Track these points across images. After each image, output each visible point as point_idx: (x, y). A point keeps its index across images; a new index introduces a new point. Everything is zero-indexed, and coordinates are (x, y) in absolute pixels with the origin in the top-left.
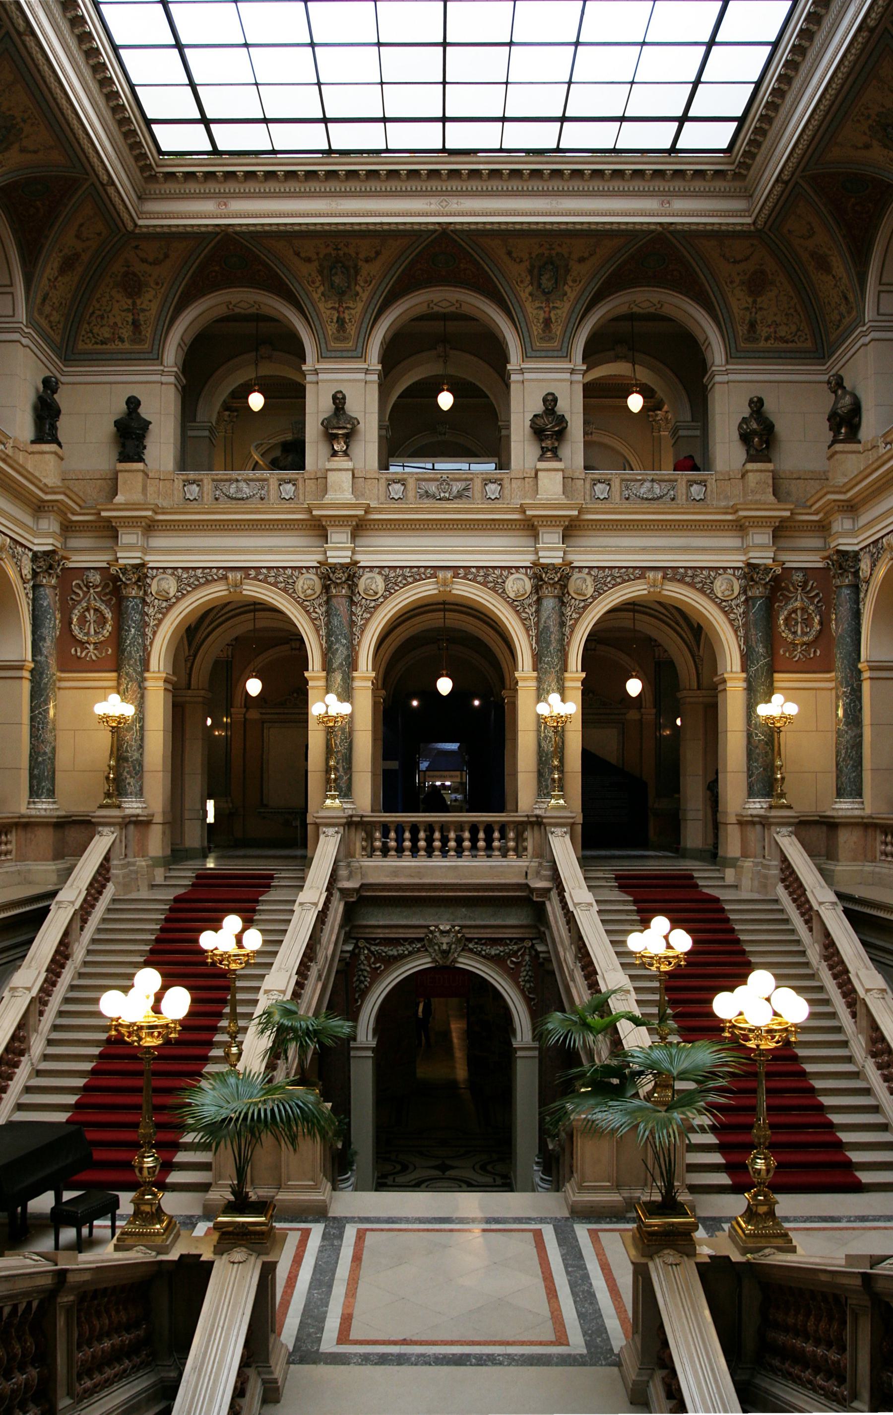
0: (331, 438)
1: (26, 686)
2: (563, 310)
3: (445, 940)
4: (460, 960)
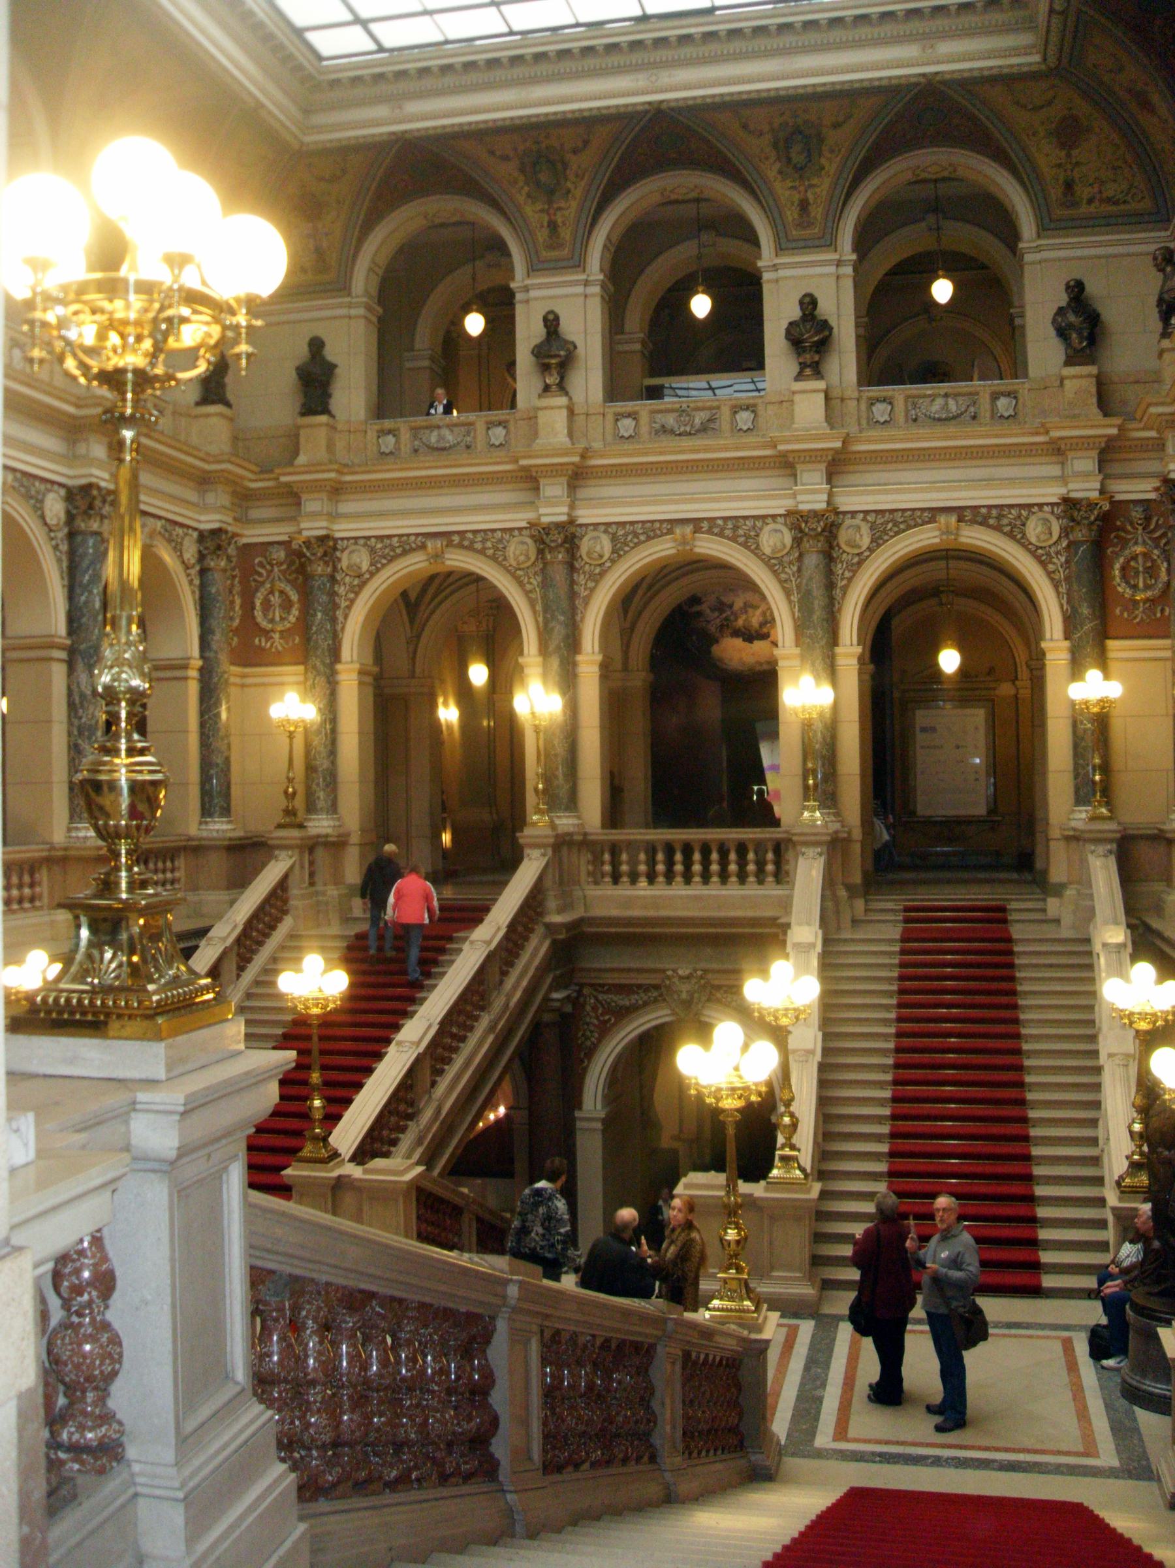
0: (545, 368)
1: (193, 688)
2: (822, 188)
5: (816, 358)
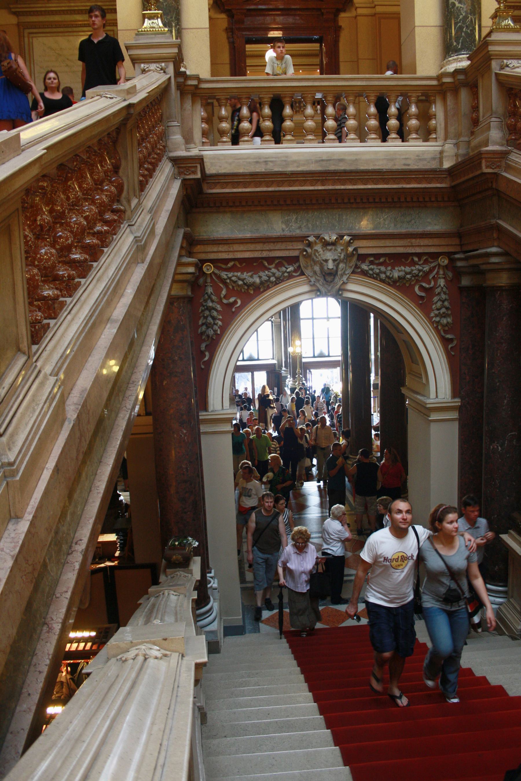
3: (329, 256)
4: (351, 286)
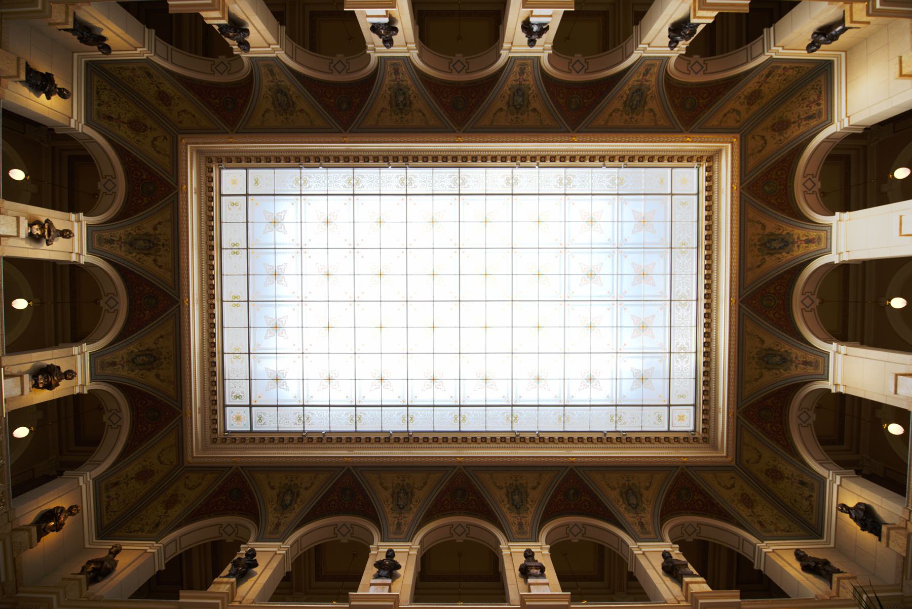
5: (41, 386)
